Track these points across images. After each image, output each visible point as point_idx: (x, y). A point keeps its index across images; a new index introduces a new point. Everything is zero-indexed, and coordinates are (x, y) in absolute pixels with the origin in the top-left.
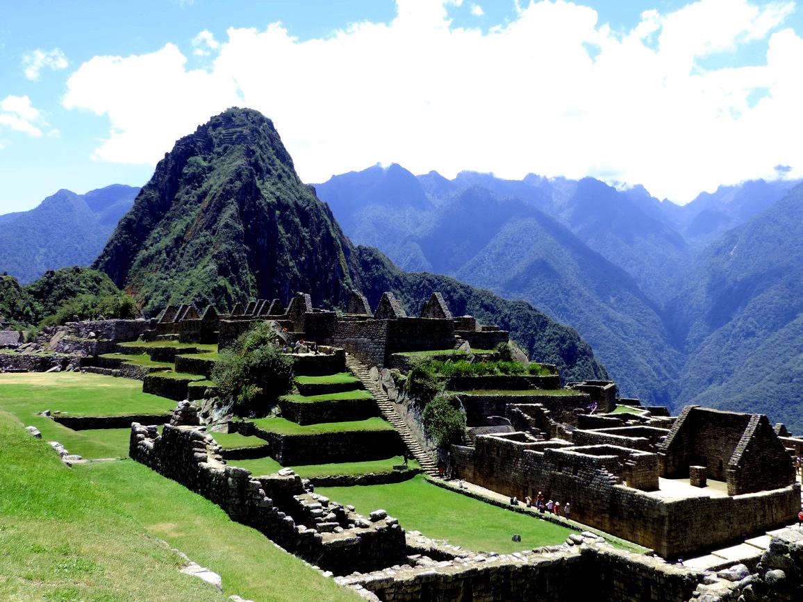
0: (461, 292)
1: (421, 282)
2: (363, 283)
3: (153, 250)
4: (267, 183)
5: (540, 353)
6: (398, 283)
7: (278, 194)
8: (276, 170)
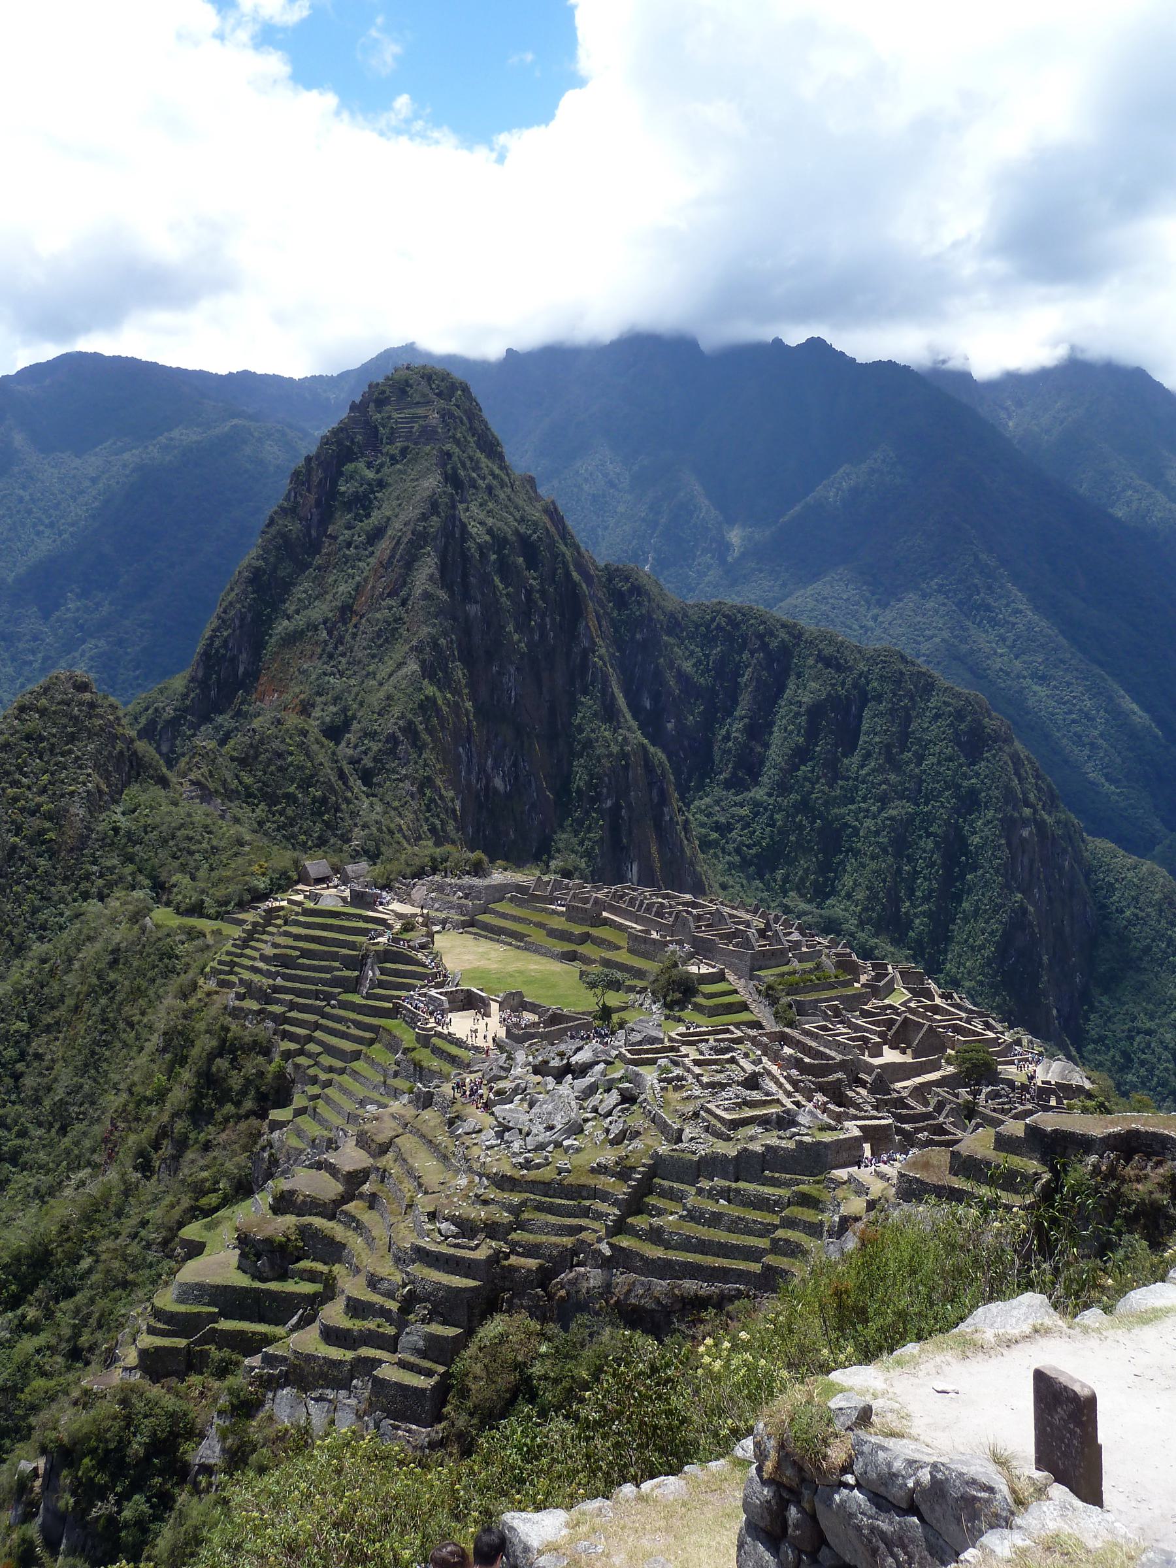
0: (783, 634)
1: (713, 619)
2: (616, 631)
3: (300, 621)
4: (473, 507)
5: (920, 740)
6: (675, 624)
7: (490, 521)
8: (484, 478)
